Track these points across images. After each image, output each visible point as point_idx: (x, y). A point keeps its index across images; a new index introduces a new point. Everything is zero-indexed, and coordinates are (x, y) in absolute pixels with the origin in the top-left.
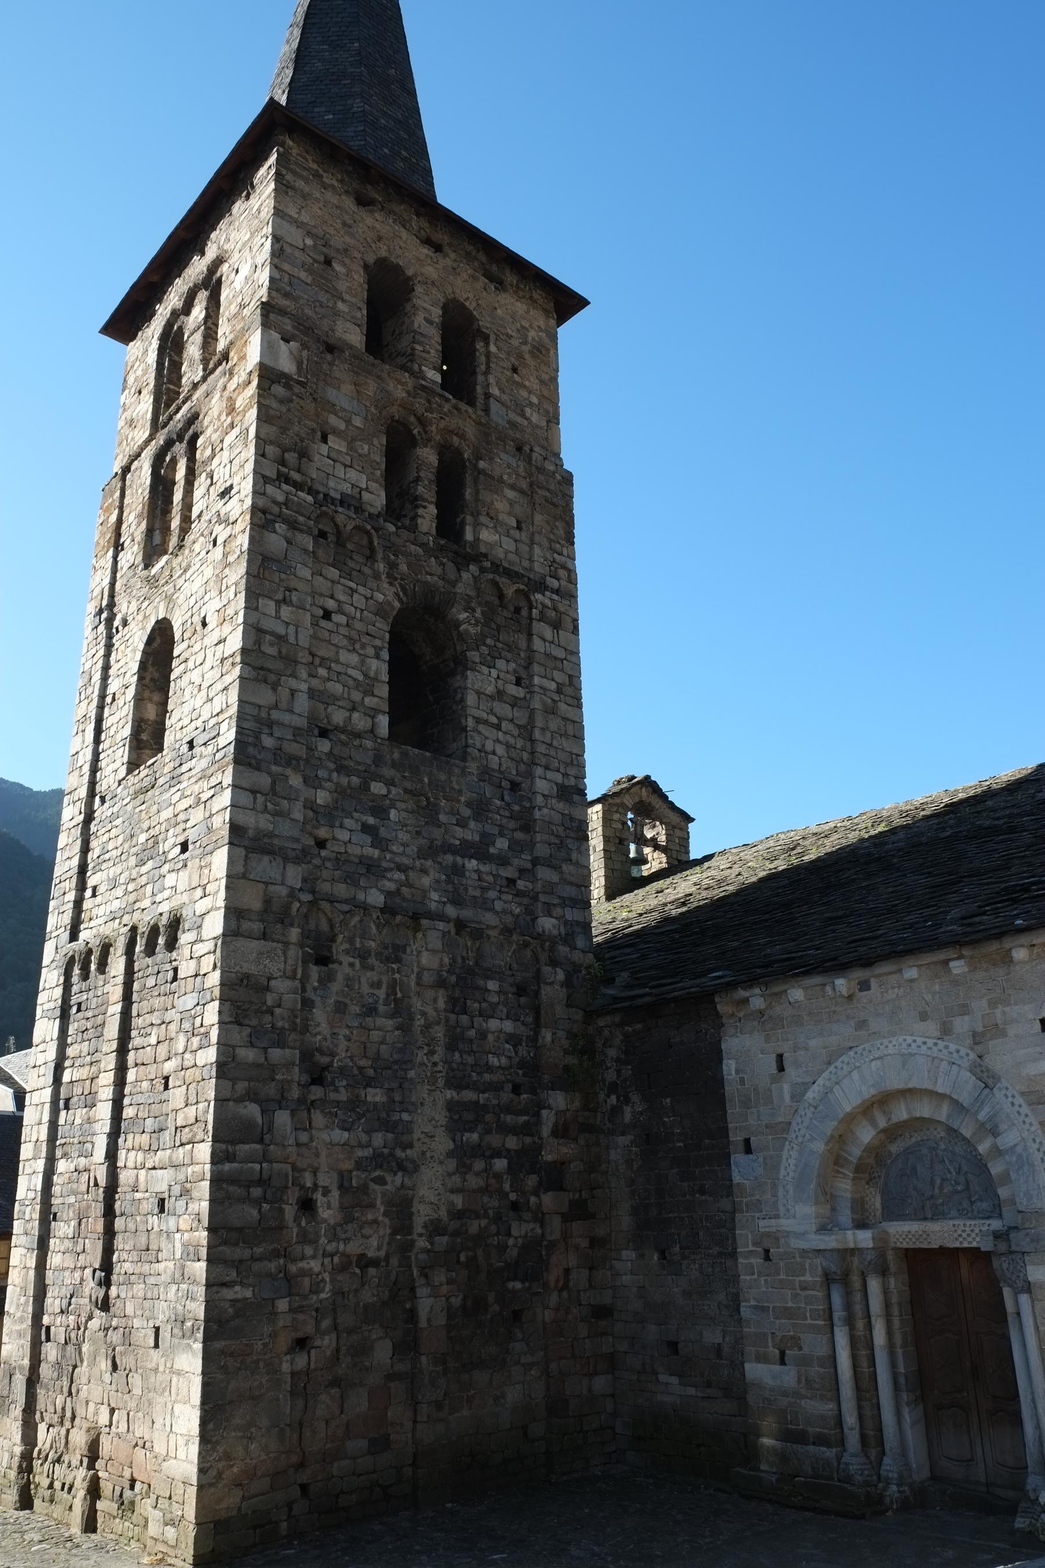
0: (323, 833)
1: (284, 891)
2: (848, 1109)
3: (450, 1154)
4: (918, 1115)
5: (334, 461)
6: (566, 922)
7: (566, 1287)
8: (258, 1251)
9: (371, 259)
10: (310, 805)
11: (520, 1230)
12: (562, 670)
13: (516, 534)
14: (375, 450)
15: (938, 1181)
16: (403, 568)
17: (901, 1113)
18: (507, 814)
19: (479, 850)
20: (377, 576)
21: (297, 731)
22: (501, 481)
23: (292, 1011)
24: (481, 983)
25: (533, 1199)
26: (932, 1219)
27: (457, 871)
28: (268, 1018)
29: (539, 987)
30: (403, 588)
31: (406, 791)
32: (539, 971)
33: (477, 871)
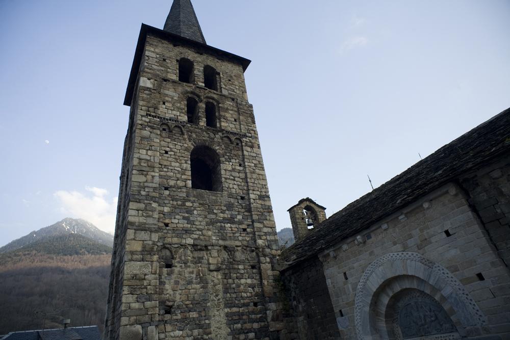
0: (167, 221)
1: (150, 243)
2: (375, 290)
4: (405, 287)
5: (168, 109)
6: (268, 241)
9: (179, 58)
10: (161, 212)
12: (256, 160)
13: (235, 123)
14: (183, 105)
15: (423, 317)
16: (194, 136)
17: (397, 288)
18: (240, 207)
19: (231, 220)
20: (184, 139)
21: (155, 189)
23: (155, 286)
24: (236, 266)
26: (425, 335)
27: (222, 228)
28: (145, 290)
29: (260, 265)
31: (200, 204)
32: (259, 260)
33: (231, 227)
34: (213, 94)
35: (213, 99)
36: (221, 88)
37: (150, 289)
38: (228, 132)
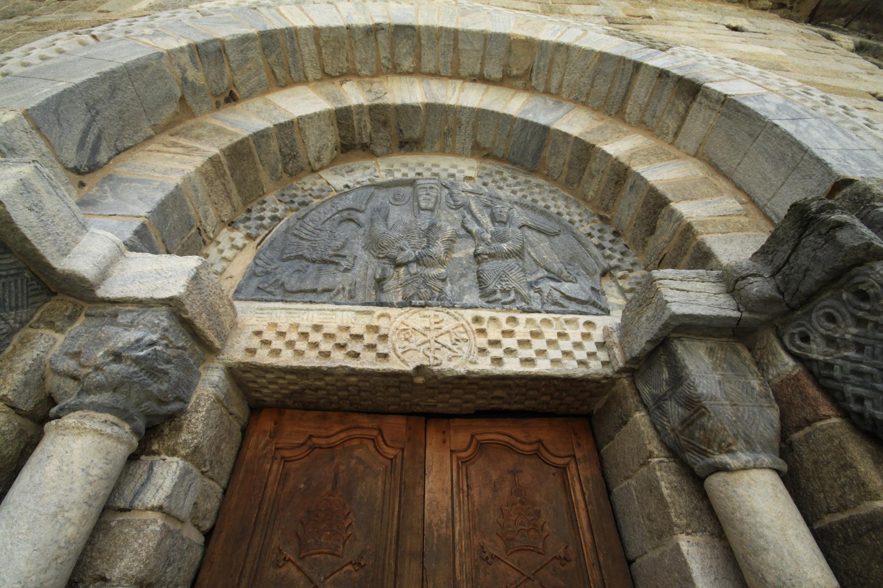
26: (407, 303)
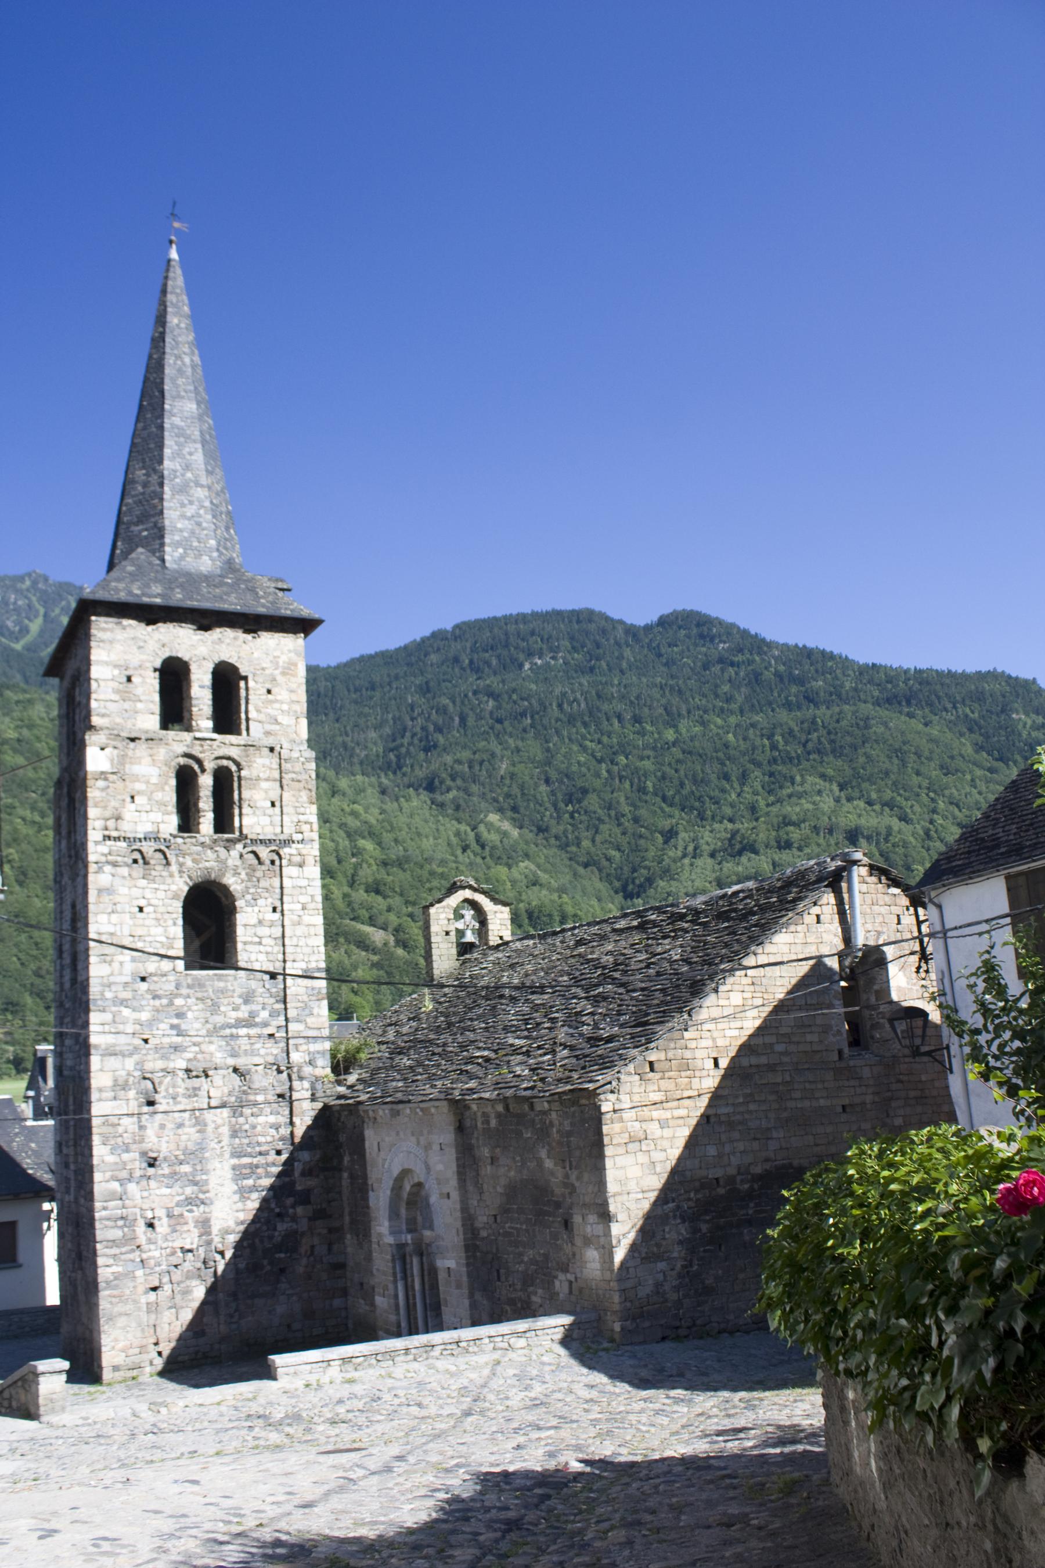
1: (124, 1073)
3: (235, 1193)
7: (312, 1253)
8: (124, 1250)
9: (158, 664)
11: (282, 1227)
13: (270, 811)
16: (189, 862)
19: (249, 1022)
22: (258, 779)
25: (291, 1211)
30: (190, 877)
34: (229, 745)
35: (229, 758)
36: (247, 719)
37: (127, 1138)
38: (254, 842)
